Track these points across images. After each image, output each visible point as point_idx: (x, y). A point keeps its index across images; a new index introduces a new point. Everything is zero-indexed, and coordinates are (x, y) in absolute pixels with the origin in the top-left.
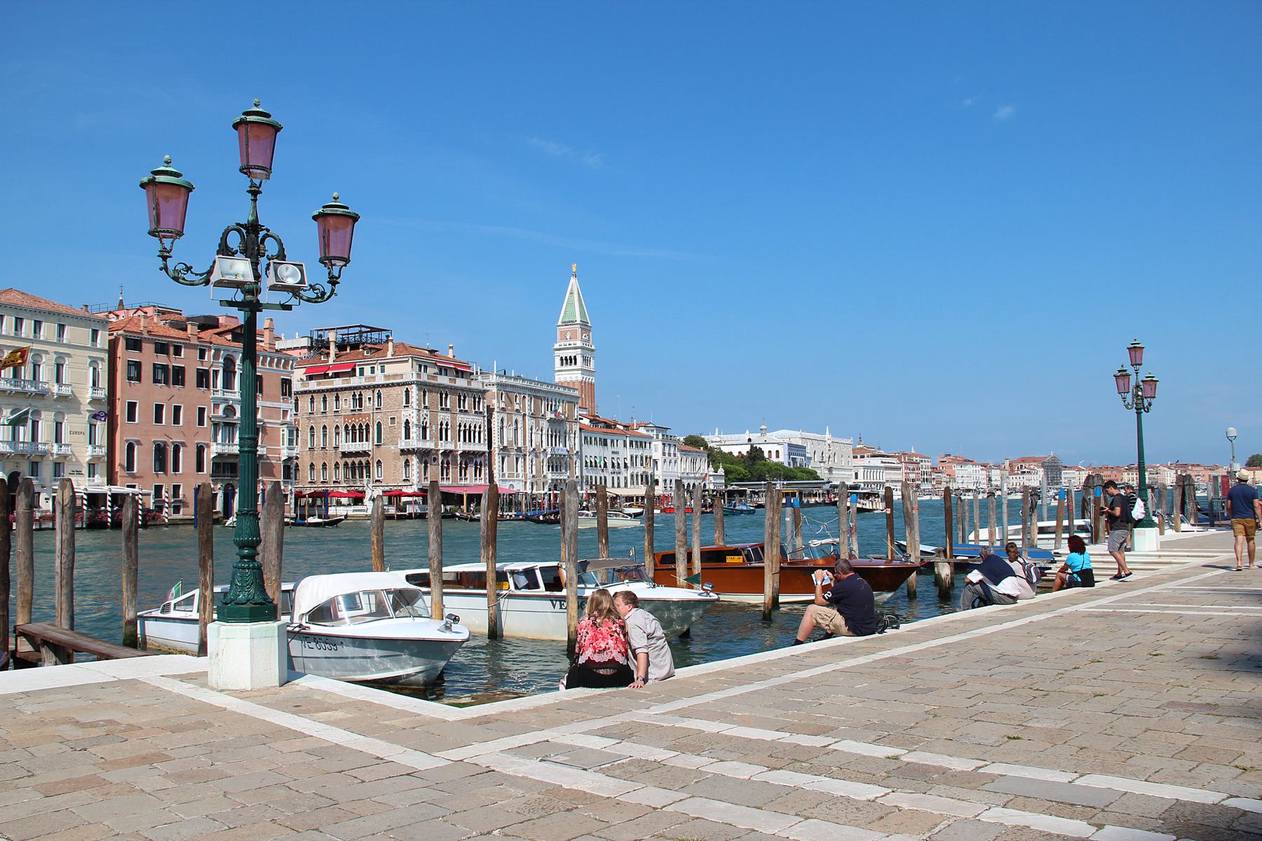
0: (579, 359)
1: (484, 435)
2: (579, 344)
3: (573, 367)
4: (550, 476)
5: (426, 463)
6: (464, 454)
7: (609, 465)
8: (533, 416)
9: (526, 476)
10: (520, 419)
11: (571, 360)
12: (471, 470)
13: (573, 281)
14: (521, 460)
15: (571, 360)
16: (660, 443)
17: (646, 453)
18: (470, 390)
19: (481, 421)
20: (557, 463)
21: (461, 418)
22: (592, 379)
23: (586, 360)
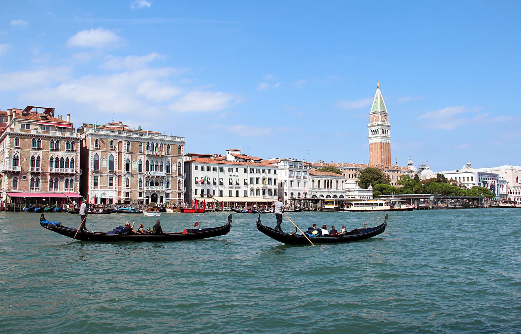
0: (380, 131)
2: (380, 123)
3: (377, 135)
4: (145, 188)
5: (15, 181)
6: (52, 174)
7: (226, 183)
8: (128, 152)
11: (375, 132)
12: (62, 183)
13: (378, 90)
14: (115, 181)
15: (375, 132)
16: (287, 171)
17: (268, 176)
19: (76, 156)
20: (153, 182)
21: (51, 154)
22: (388, 141)
23: (384, 131)
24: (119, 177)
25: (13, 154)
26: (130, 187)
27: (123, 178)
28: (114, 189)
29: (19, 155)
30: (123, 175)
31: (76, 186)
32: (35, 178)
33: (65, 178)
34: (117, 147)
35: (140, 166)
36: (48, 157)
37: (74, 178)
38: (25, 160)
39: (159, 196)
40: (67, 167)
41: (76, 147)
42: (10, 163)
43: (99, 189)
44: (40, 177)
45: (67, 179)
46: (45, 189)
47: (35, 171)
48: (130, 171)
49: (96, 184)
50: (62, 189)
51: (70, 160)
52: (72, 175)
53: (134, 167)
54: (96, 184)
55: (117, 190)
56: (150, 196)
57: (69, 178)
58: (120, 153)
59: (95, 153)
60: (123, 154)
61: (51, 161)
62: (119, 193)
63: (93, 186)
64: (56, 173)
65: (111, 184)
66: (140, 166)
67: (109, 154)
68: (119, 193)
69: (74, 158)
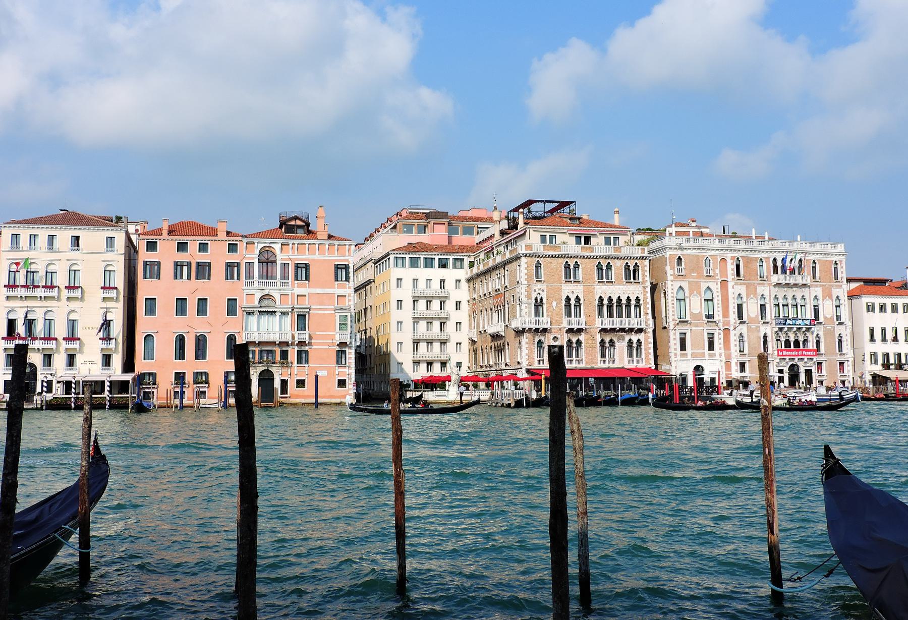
1: (646, 306)
9: (728, 357)
10: (716, 287)
12: (621, 346)
24: (726, 331)
25: (534, 295)
26: (746, 351)
27: (732, 333)
28: (717, 357)
29: (544, 295)
30: (731, 328)
31: (647, 354)
32: (574, 340)
33: (627, 339)
34: (718, 271)
35: (763, 306)
36: (594, 297)
37: (641, 336)
38: (554, 304)
39: (802, 369)
40: (629, 315)
41: (643, 275)
42: (530, 312)
43: (689, 357)
45: (630, 341)
46: (593, 360)
47: (575, 327)
48: (745, 318)
49: (683, 347)
50: (621, 359)
51: (633, 302)
52: (640, 331)
53: (751, 310)
54: (683, 347)
55: (723, 358)
56: (786, 369)
57: (634, 338)
58: (724, 283)
59: (677, 285)
60: (730, 285)
61: (601, 305)
62: (728, 365)
63: (678, 351)
64: (611, 329)
65: (711, 347)
66: (763, 306)
67: (704, 287)
68: (728, 365)
69: (641, 298)
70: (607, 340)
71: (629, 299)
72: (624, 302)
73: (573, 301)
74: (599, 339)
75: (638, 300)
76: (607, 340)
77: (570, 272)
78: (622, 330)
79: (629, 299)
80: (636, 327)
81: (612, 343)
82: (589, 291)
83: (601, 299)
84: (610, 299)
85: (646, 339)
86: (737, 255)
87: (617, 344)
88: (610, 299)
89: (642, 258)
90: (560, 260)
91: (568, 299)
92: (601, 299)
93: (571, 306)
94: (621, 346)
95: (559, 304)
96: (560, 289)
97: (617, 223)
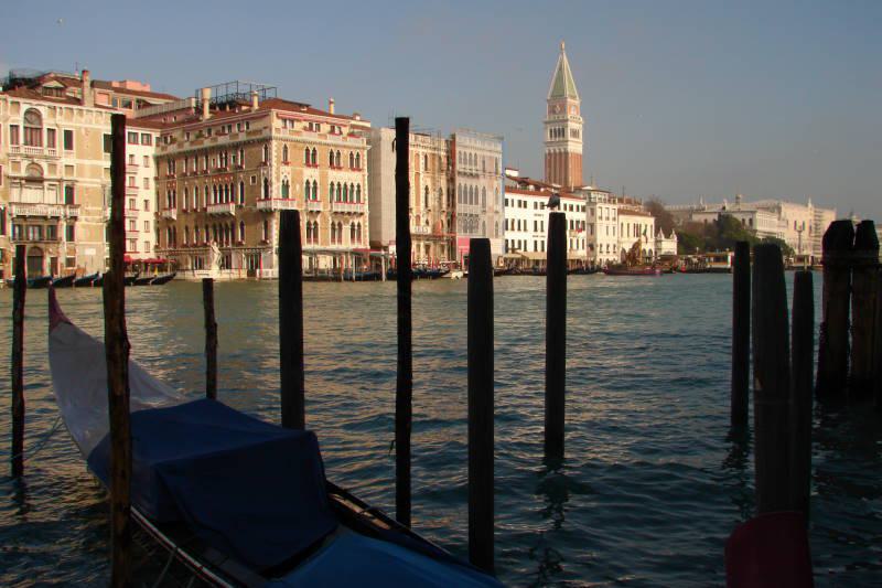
7: (530, 226)
12: (346, 229)
18: (345, 147)
25: (282, 177)
29: (289, 178)
32: (312, 222)
37: (361, 220)
44: (318, 220)
45: (353, 225)
50: (347, 241)
51: (356, 189)
52: (362, 214)
60: (422, 176)
70: (336, 223)
71: (352, 186)
72: (349, 187)
73: (312, 185)
74: (330, 222)
75: (359, 186)
76: (336, 223)
77: (311, 160)
78: (349, 213)
79: (352, 186)
80: (359, 211)
81: (340, 225)
82: (324, 176)
83: (332, 184)
84: (339, 185)
85: (364, 222)
86: (425, 151)
87: (344, 227)
88: (339, 185)
89: (363, 148)
90: (301, 145)
91: (308, 182)
92: (332, 184)
93: (311, 189)
94: (346, 229)
95: (301, 186)
96: (301, 173)
97: (332, 112)
